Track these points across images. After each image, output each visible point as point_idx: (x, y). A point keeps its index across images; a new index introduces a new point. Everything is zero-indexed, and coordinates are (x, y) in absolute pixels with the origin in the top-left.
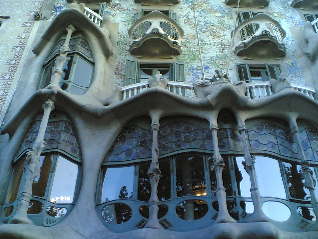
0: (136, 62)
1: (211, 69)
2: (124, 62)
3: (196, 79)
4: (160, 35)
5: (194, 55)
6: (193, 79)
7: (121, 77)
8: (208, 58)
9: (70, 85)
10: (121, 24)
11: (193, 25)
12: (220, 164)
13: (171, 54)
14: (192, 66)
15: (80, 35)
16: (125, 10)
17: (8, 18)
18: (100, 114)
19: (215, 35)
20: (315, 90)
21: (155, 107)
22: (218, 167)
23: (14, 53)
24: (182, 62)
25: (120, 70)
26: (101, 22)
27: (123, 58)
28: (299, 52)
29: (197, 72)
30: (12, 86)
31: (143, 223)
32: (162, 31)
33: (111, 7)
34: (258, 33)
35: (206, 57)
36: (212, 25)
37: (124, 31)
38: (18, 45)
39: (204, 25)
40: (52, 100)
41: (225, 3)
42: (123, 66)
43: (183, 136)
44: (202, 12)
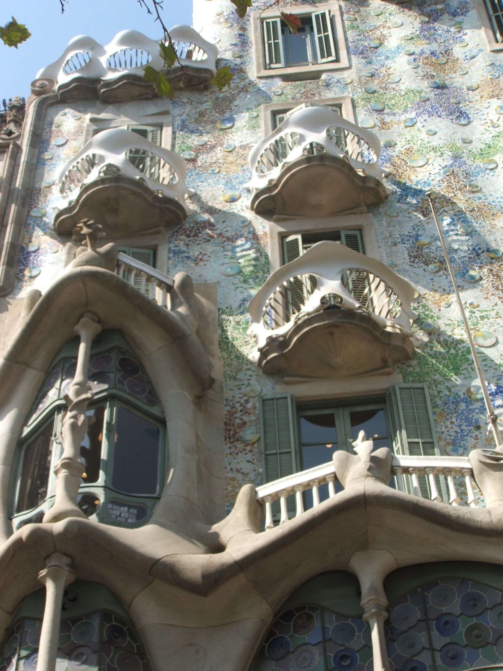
0: (286, 398)
2: (247, 402)
3: (470, 431)
5: (452, 354)
6: (462, 430)
7: (244, 450)
11: (435, 263)
14: (453, 390)
15: (117, 341)
29: (470, 407)
33: (188, 236)
36: (492, 258)
39: (470, 258)
42: (246, 412)
43: (462, 629)
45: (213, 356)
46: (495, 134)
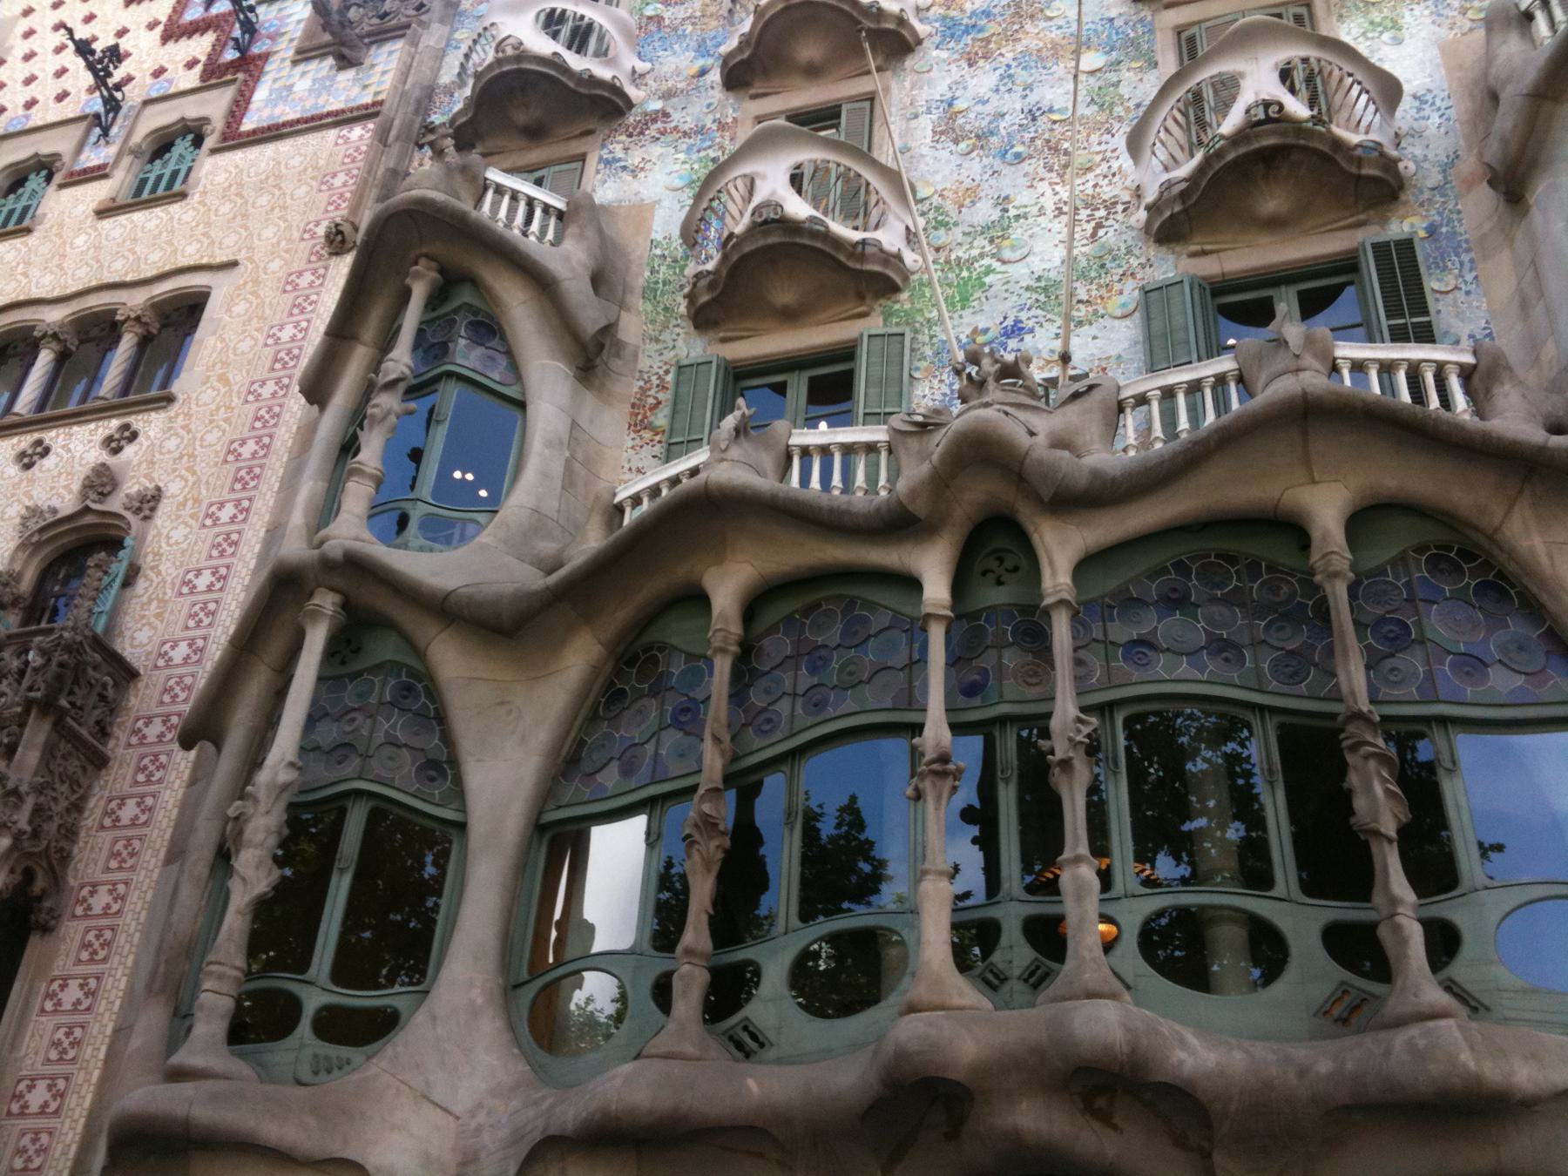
1: (1032, 331)
2: (667, 372)
8: (1024, 284)
9: (417, 513)
10: (665, 203)
12: (935, 767)
13: (861, 297)
15: (466, 296)
16: (685, 134)
17: (233, 264)
19: (1066, 166)
20: (1475, 353)
21: (719, 553)
23: (251, 408)
26: (561, 215)
28: (1469, 164)
30: (243, 549)
32: (798, 208)
33: (630, 136)
34: (1231, 123)
35: (1013, 280)
36: (1055, 122)
38: (266, 375)
43: (835, 665)
44: (1014, 64)
45: (628, 310)
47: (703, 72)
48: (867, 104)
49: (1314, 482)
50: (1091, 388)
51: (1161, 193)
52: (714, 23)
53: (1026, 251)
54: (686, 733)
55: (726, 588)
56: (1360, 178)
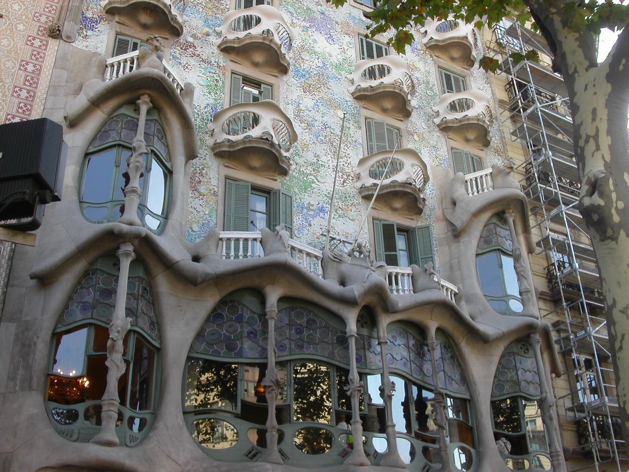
2: (203, 169)
4: (272, 145)
13: (275, 171)
18: (200, 279)
22: (356, 392)
23: (17, 101)
24: (290, 191)
25: (198, 183)
26: (182, 90)
27: (202, 159)
28: (439, 213)
31: (253, 453)
33: (182, 49)
36: (332, 133)
37: (203, 106)
40: (132, 244)
41: (352, 94)
46: (344, 57)
47: (208, 35)
48: (270, 87)
49: (432, 319)
50: (381, 266)
51: (371, 186)
52: (211, 13)
53: (325, 180)
54: (253, 342)
55: (273, 296)
56: (419, 207)
